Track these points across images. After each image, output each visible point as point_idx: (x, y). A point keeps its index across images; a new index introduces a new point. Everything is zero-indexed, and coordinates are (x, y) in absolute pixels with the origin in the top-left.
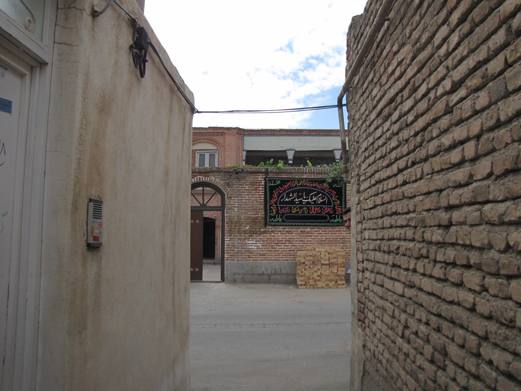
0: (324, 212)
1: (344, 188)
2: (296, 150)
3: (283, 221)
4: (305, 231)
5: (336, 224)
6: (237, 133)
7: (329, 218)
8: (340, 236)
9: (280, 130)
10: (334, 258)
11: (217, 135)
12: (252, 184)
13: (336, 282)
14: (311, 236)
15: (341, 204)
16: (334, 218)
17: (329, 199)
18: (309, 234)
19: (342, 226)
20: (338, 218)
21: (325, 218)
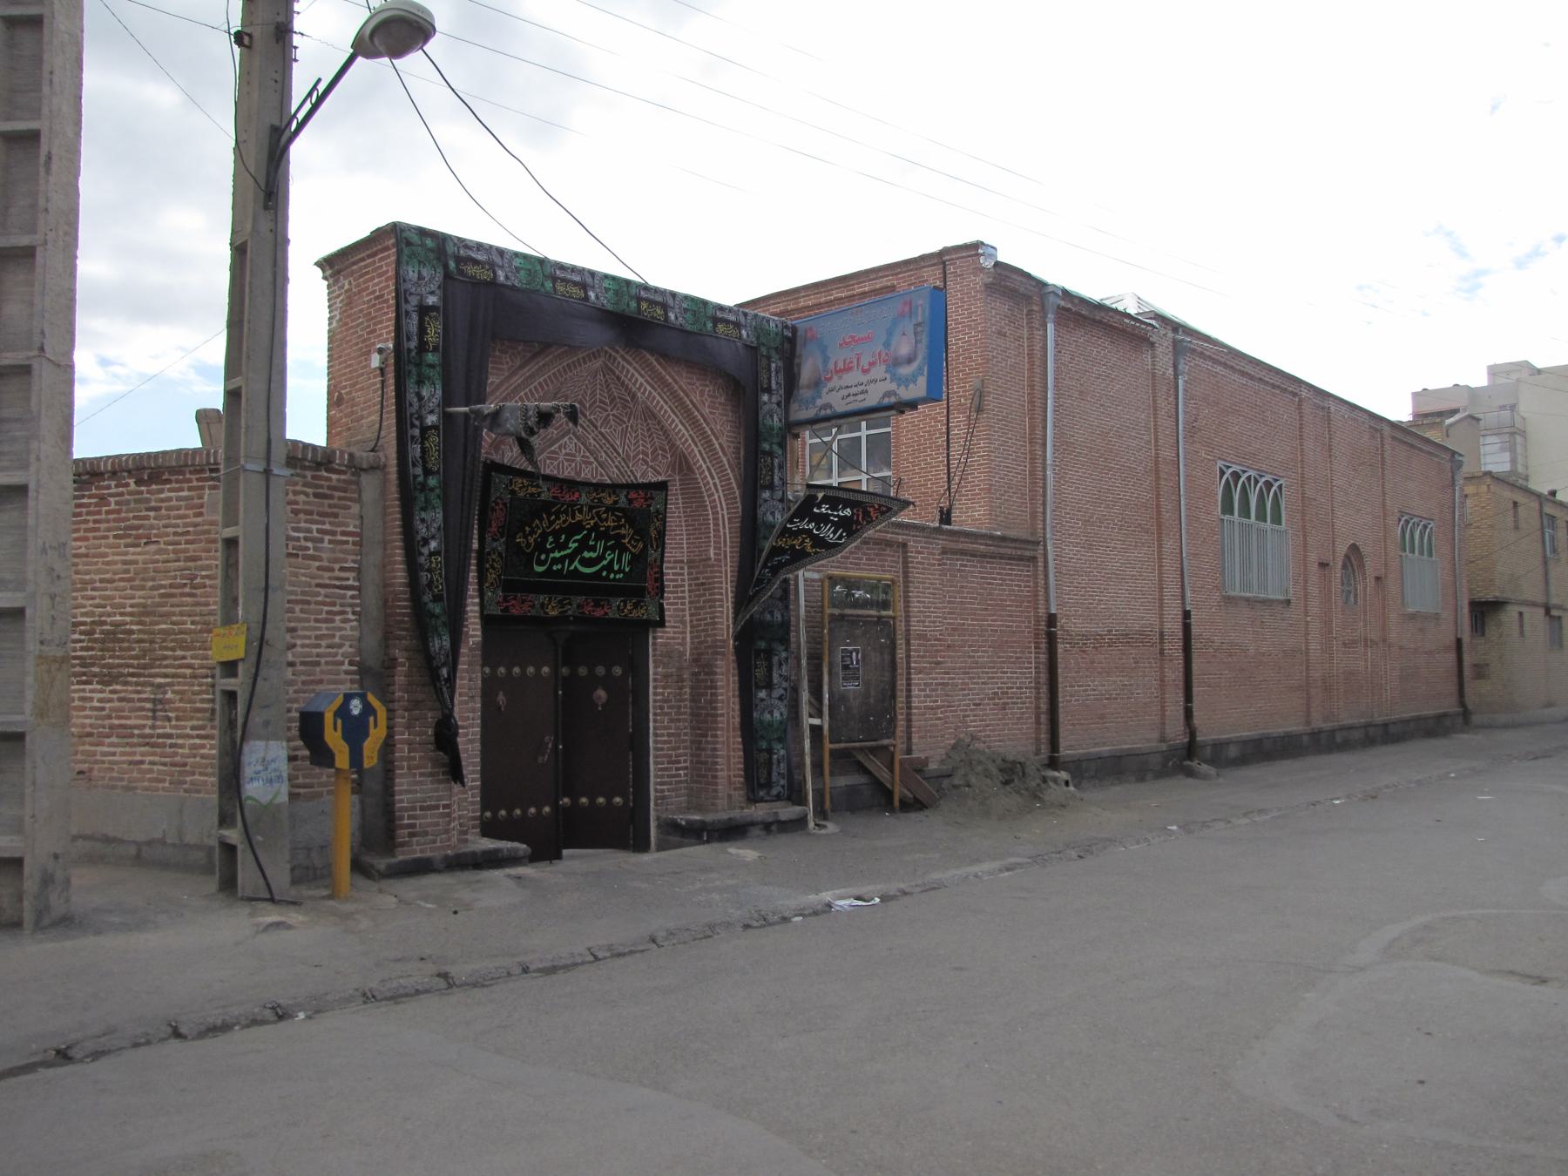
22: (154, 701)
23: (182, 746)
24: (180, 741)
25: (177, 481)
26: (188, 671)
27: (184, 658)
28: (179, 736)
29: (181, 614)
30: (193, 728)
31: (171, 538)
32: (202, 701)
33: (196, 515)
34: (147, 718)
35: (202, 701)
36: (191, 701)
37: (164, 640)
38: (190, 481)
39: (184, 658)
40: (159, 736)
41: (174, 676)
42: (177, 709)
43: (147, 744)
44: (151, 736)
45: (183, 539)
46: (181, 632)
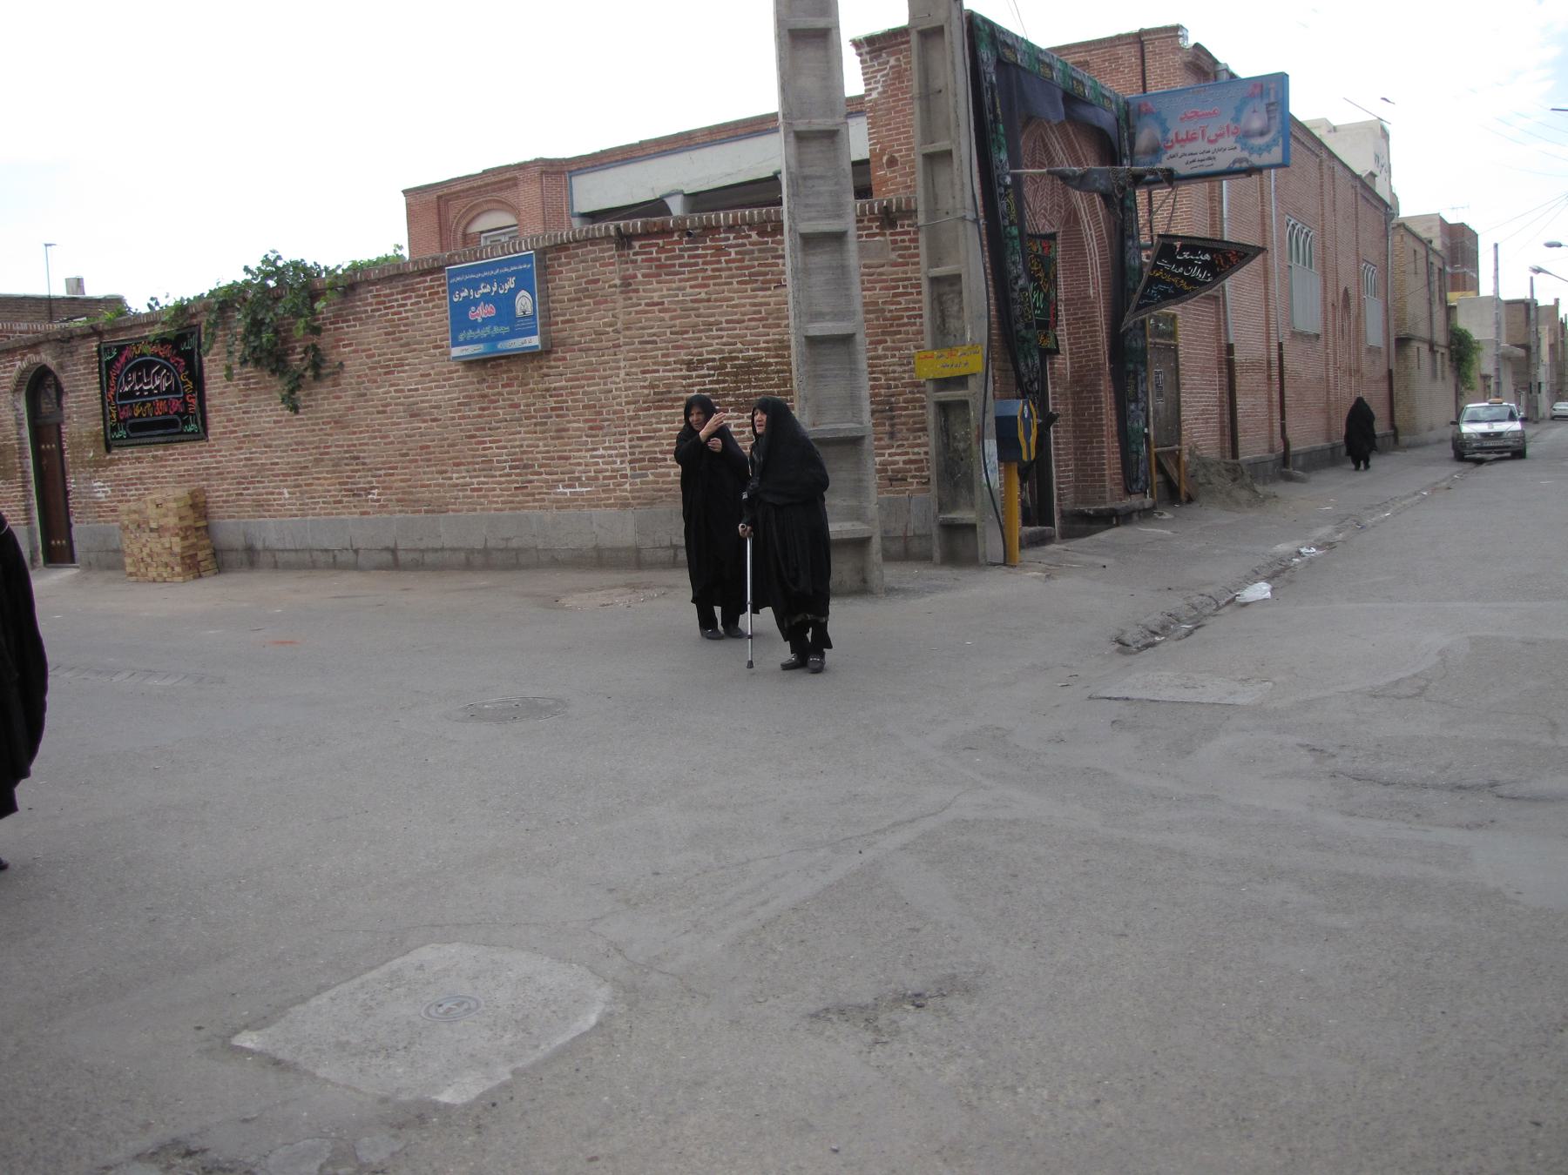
3: (128, 437)
11: (508, 187)
12: (88, 360)
16: (186, 423)
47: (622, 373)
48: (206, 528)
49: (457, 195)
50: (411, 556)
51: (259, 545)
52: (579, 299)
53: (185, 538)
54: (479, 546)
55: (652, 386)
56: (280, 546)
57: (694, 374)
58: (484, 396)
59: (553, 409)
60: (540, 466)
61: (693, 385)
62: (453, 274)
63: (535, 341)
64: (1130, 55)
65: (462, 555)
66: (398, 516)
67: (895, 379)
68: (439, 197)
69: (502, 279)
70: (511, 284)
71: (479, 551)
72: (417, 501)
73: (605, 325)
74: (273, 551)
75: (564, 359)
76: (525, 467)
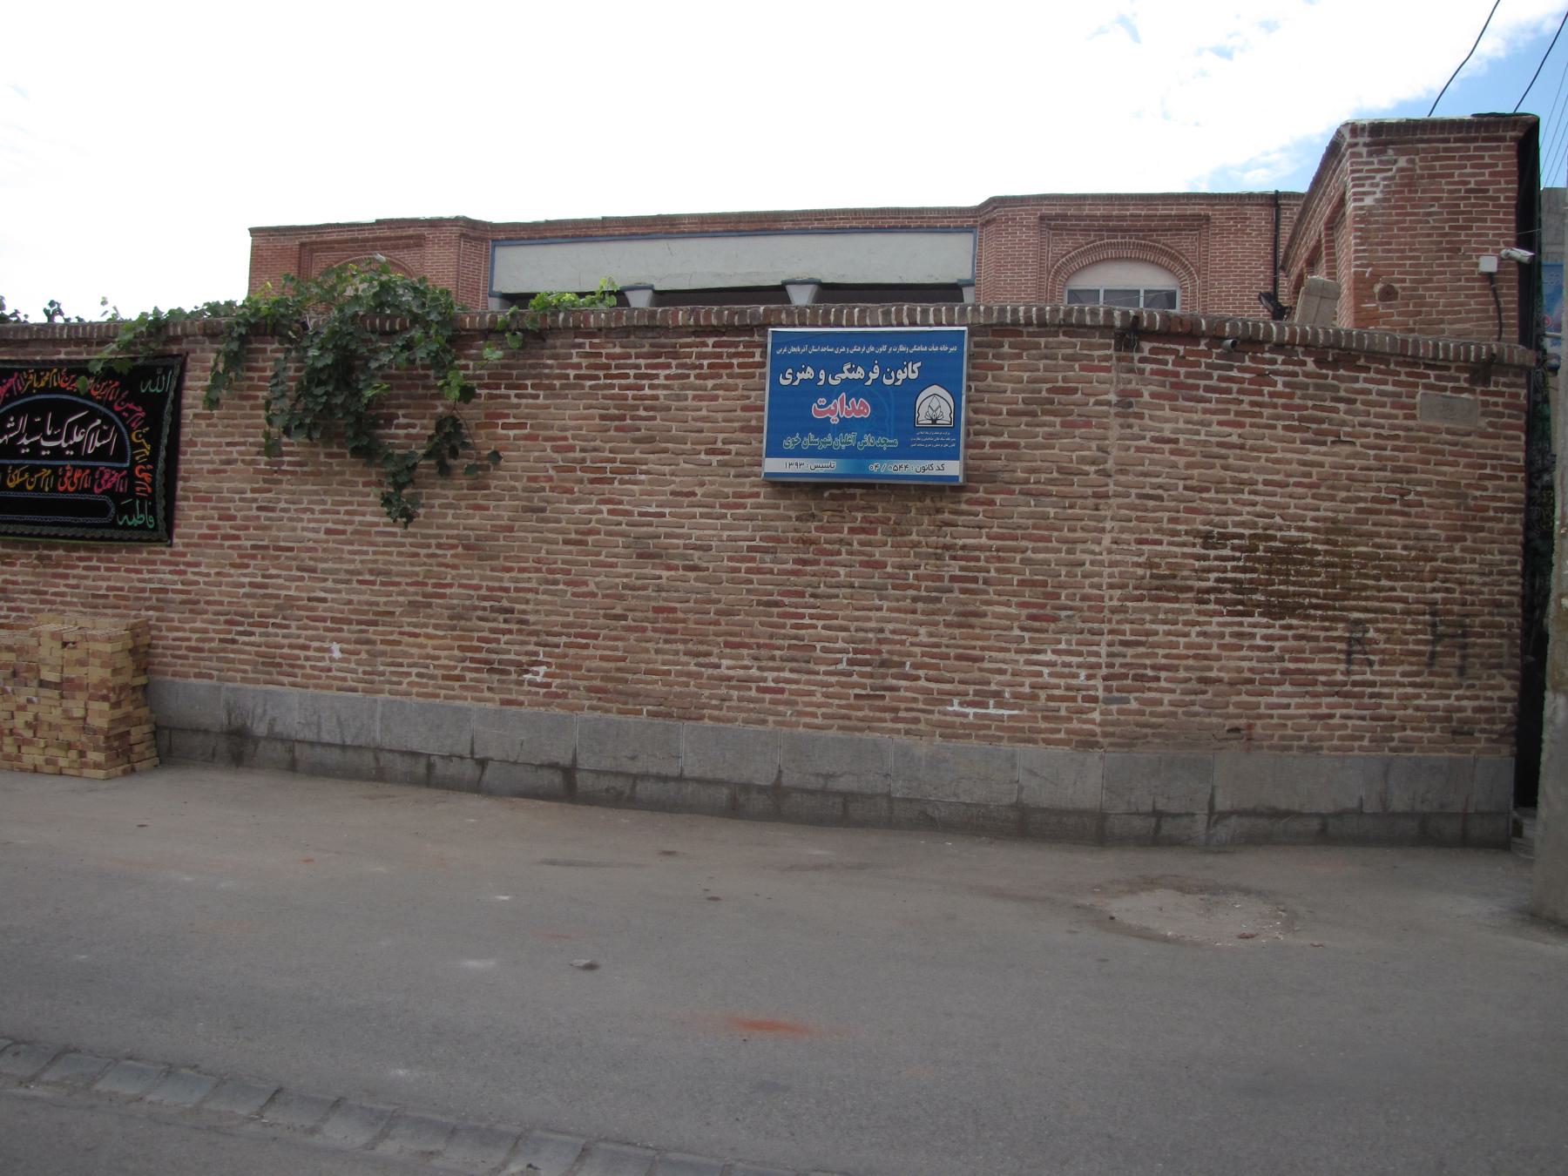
0: (100, 486)
1: (172, 394)
2: (657, 288)
4: (49, 557)
5: (137, 534)
6: (462, 235)
7: (113, 510)
8: (150, 581)
9: (604, 219)
10: (82, 663)
11: (408, 247)
13: (82, 754)
14: (66, 576)
15: (153, 459)
16: (130, 511)
17: (120, 440)
18: (61, 570)
19: (159, 541)
20: (142, 511)
21: (100, 509)
22: (1349, 641)
23: (1390, 696)
24: (1386, 690)
25: (1378, 371)
26: (1399, 606)
27: (1393, 589)
28: (1384, 684)
29: (1389, 536)
30: (1404, 674)
31: (1371, 440)
32: (1418, 642)
33: (1406, 417)
34: (1338, 661)
35: (1418, 642)
36: (1401, 642)
37: (1364, 566)
38: (1398, 374)
39: (1393, 589)
40: (1355, 684)
41: (1375, 611)
42: (1383, 652)
43: (1337, 694)
44: (1345, 684)
45: (1390, 443)
46: (1388, 558)
47: (1107, 540)
48: (145, 687)
49: (329, 246)
50: (604, 783)
51: (261, 729)
52: (1033, 414)
53: (116, 705)
54: (764, 777)
55: (1150, 565)
56: (310, 735)
57: (1212, 553)
58: (808, 542)
59: (953, 579)
60: (915, 666)
61: (1209, 570)
62: (780, 340)
63: (953, 468)
64: (1260, 218)
65: (724, 793)
66: (587, 714)
67: (1472, 593)
68: (302, 245)
69: (899, 362)
70: (911, 372)
71: (762, 790)
72: (636, 695)
73: (1082, 460)
74: (290, 742)
75: (992, 503)
76: (883, 664)
